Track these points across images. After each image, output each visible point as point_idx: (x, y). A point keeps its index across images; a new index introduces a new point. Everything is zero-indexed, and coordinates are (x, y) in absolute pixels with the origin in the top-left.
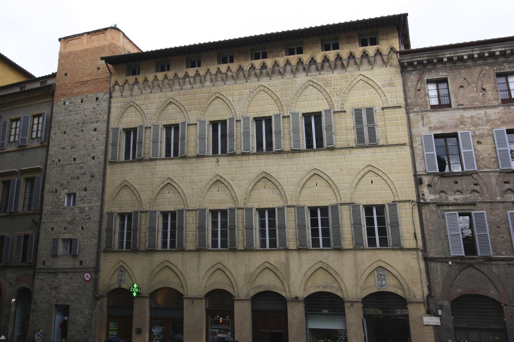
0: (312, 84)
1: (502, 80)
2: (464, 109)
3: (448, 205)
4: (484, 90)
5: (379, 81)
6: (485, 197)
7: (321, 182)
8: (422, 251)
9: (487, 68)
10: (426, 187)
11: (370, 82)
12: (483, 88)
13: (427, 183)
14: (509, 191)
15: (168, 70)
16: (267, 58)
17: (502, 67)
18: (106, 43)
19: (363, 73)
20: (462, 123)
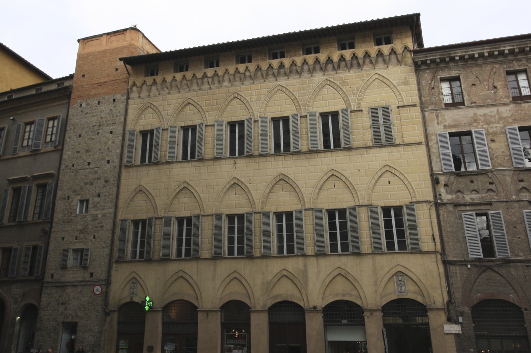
0: (329, 83)
1: (512, 78)
2: (477, 107)
3: (465, 205)
4: (495, 87)
5: (394, 80)
6: (500, 196)
7: (339, 184)
8: (440, 254)
9: (497, 66)
10: (443, 187)
11: (385, 81)
12: (494, 86)
13: (443, 183)
14: (524, 190)
15: (187, 70)
16: (284, 57)
17: (511, 65)
18: (125, 44)
19: (378, 72)
20: (475, 121)
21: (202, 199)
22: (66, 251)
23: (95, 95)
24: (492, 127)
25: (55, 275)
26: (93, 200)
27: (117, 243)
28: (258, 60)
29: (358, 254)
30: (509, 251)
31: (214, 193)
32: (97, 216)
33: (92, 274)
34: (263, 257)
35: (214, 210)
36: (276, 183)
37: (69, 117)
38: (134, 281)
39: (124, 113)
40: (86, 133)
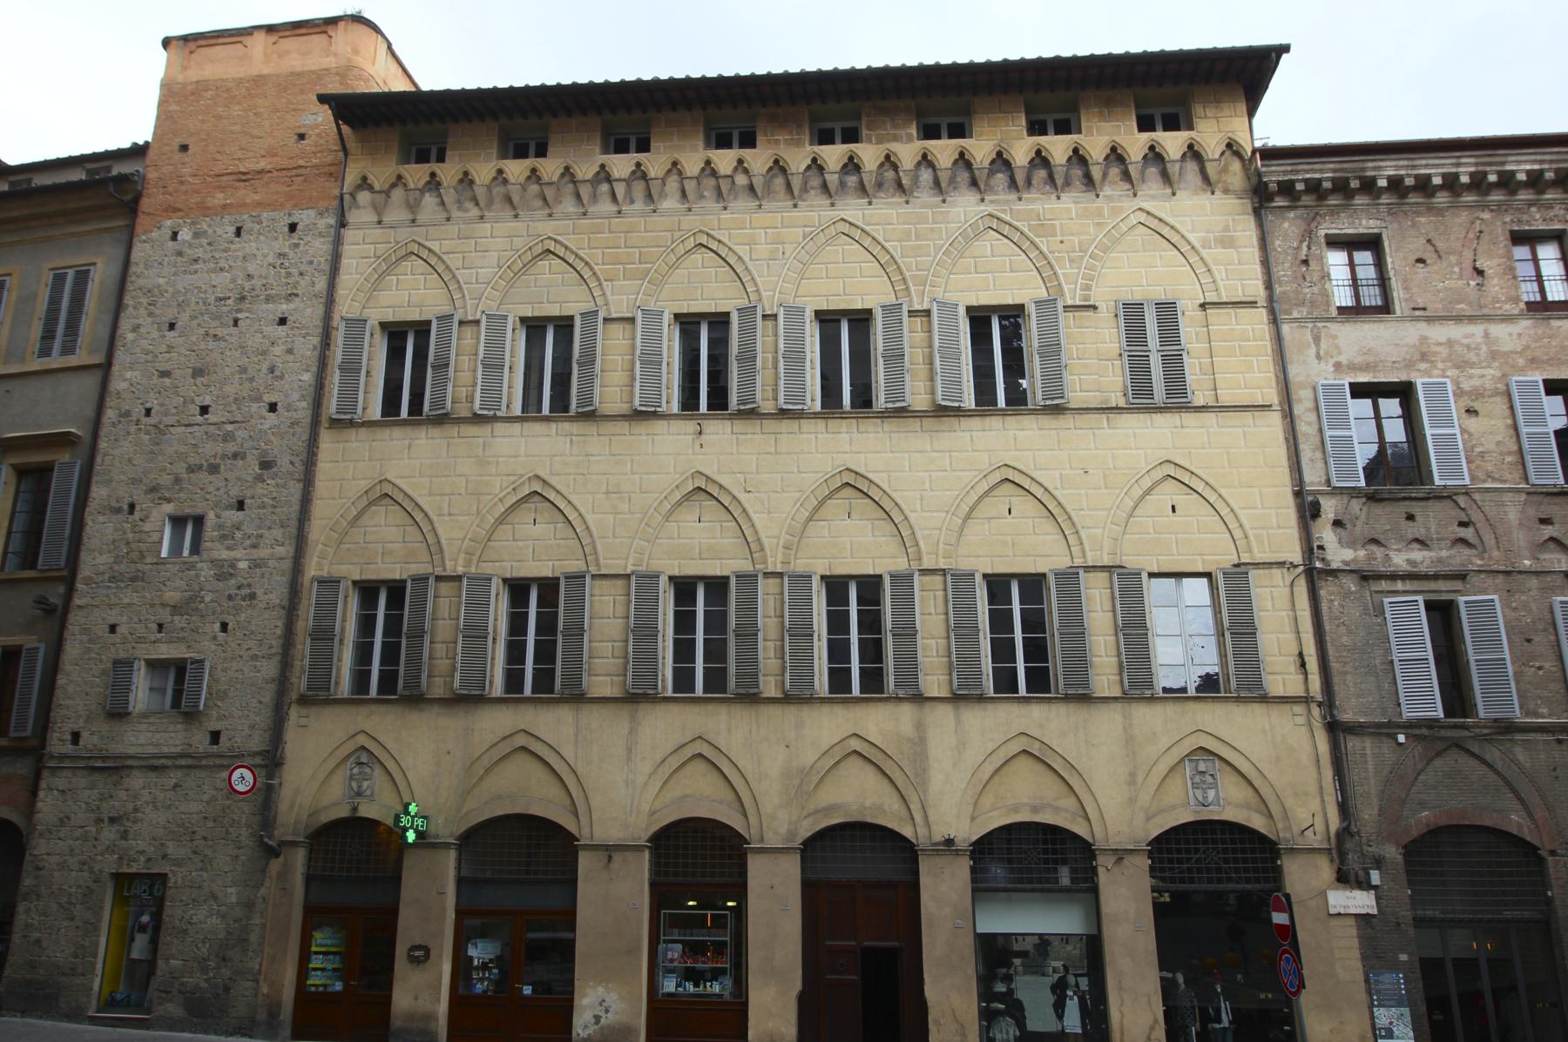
0: (997, 225)
1: (1522, 252)
2: (1430, 320)
3: (1393, 577)
4: (1480, 273)
5: (1193, 231)
6: (1490, 558)
7: (1023, 504)
8: (1320, 705)
9: (1486, 216)
10: (1329, 526)
11: (1165, 231)
12: (1475, 269)
13: (1331, 516)
14: (1552, 545)
17: (1525, 217)
18: (330, 62)
19: (1145, 205)
20: (1424, 357)
21: (593, 528)
22: (123, 667)
23: (224, 207)
24: (1471, 377)
25: (85, 735)
26: (218, 516)
27: (304, 647)
28: (777, 142)
29: (1084, 698)
30: (1516, 701)
31: (630, 512)
32: (233, 566)
33: (215, 737)
34: (787, 699)
35: (631, 561)
36: (829, 497)
37: (133, 269)
38: (364, 759)
39: (326, 267)
40: (193, 318)
